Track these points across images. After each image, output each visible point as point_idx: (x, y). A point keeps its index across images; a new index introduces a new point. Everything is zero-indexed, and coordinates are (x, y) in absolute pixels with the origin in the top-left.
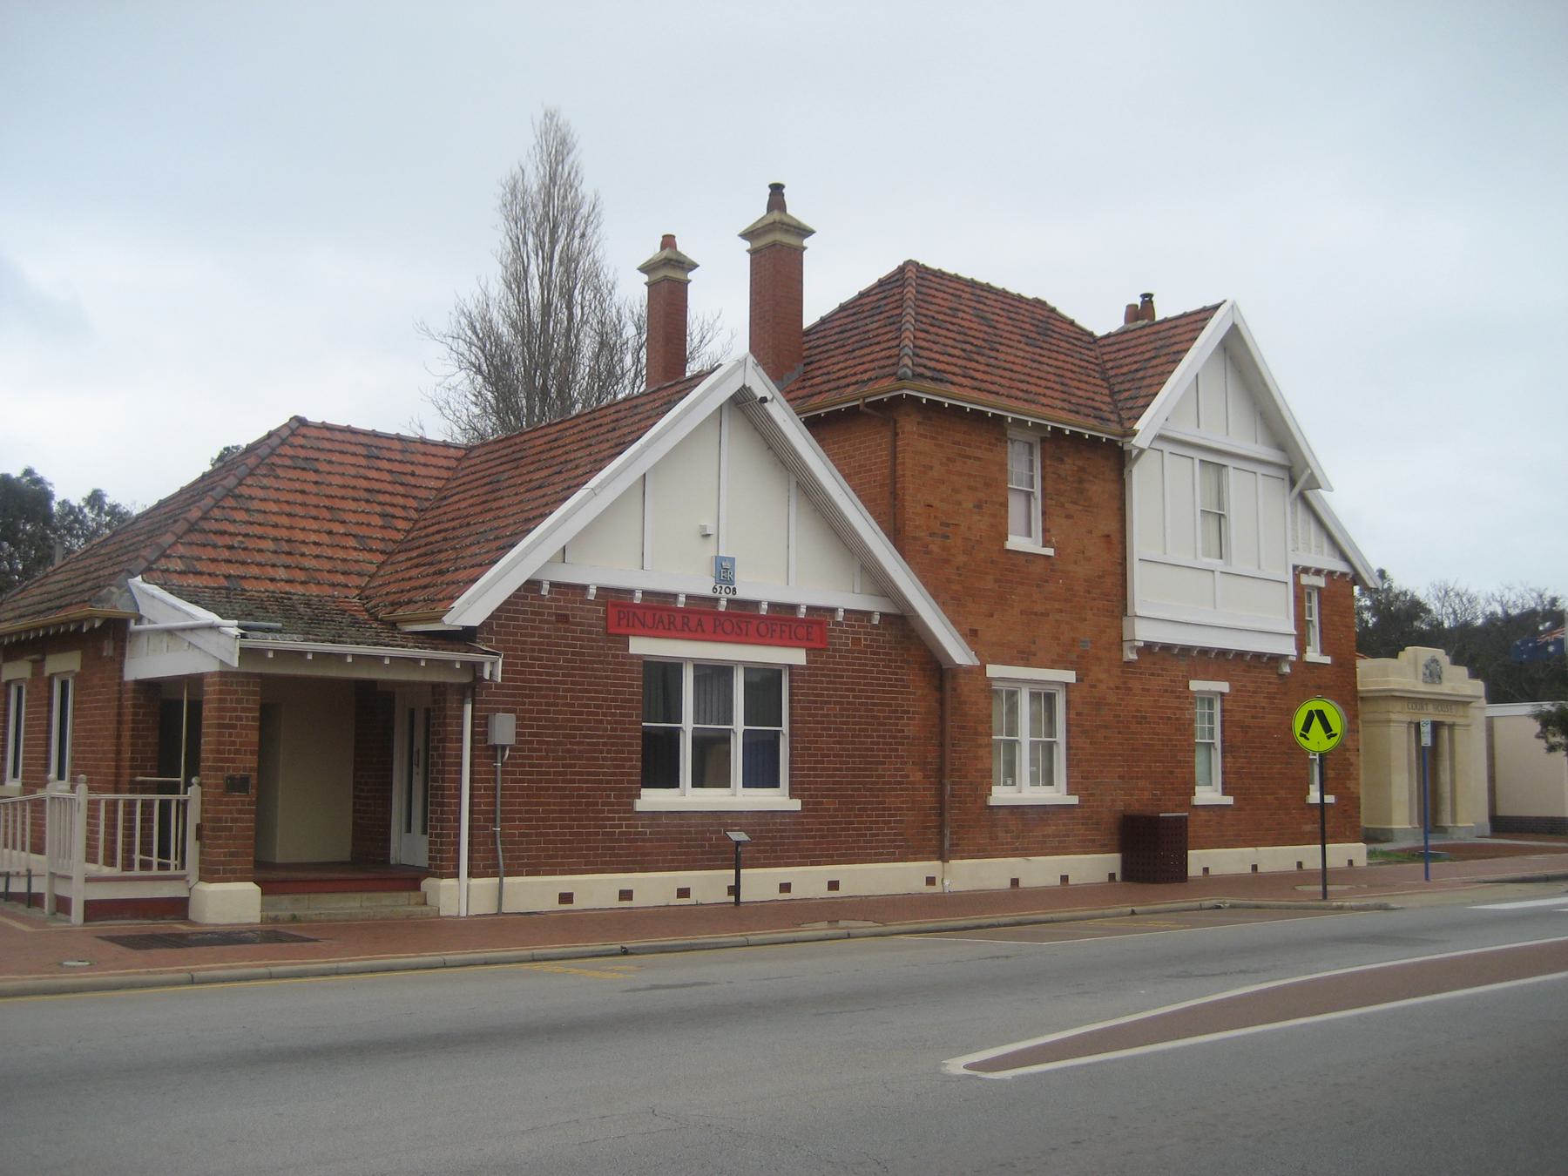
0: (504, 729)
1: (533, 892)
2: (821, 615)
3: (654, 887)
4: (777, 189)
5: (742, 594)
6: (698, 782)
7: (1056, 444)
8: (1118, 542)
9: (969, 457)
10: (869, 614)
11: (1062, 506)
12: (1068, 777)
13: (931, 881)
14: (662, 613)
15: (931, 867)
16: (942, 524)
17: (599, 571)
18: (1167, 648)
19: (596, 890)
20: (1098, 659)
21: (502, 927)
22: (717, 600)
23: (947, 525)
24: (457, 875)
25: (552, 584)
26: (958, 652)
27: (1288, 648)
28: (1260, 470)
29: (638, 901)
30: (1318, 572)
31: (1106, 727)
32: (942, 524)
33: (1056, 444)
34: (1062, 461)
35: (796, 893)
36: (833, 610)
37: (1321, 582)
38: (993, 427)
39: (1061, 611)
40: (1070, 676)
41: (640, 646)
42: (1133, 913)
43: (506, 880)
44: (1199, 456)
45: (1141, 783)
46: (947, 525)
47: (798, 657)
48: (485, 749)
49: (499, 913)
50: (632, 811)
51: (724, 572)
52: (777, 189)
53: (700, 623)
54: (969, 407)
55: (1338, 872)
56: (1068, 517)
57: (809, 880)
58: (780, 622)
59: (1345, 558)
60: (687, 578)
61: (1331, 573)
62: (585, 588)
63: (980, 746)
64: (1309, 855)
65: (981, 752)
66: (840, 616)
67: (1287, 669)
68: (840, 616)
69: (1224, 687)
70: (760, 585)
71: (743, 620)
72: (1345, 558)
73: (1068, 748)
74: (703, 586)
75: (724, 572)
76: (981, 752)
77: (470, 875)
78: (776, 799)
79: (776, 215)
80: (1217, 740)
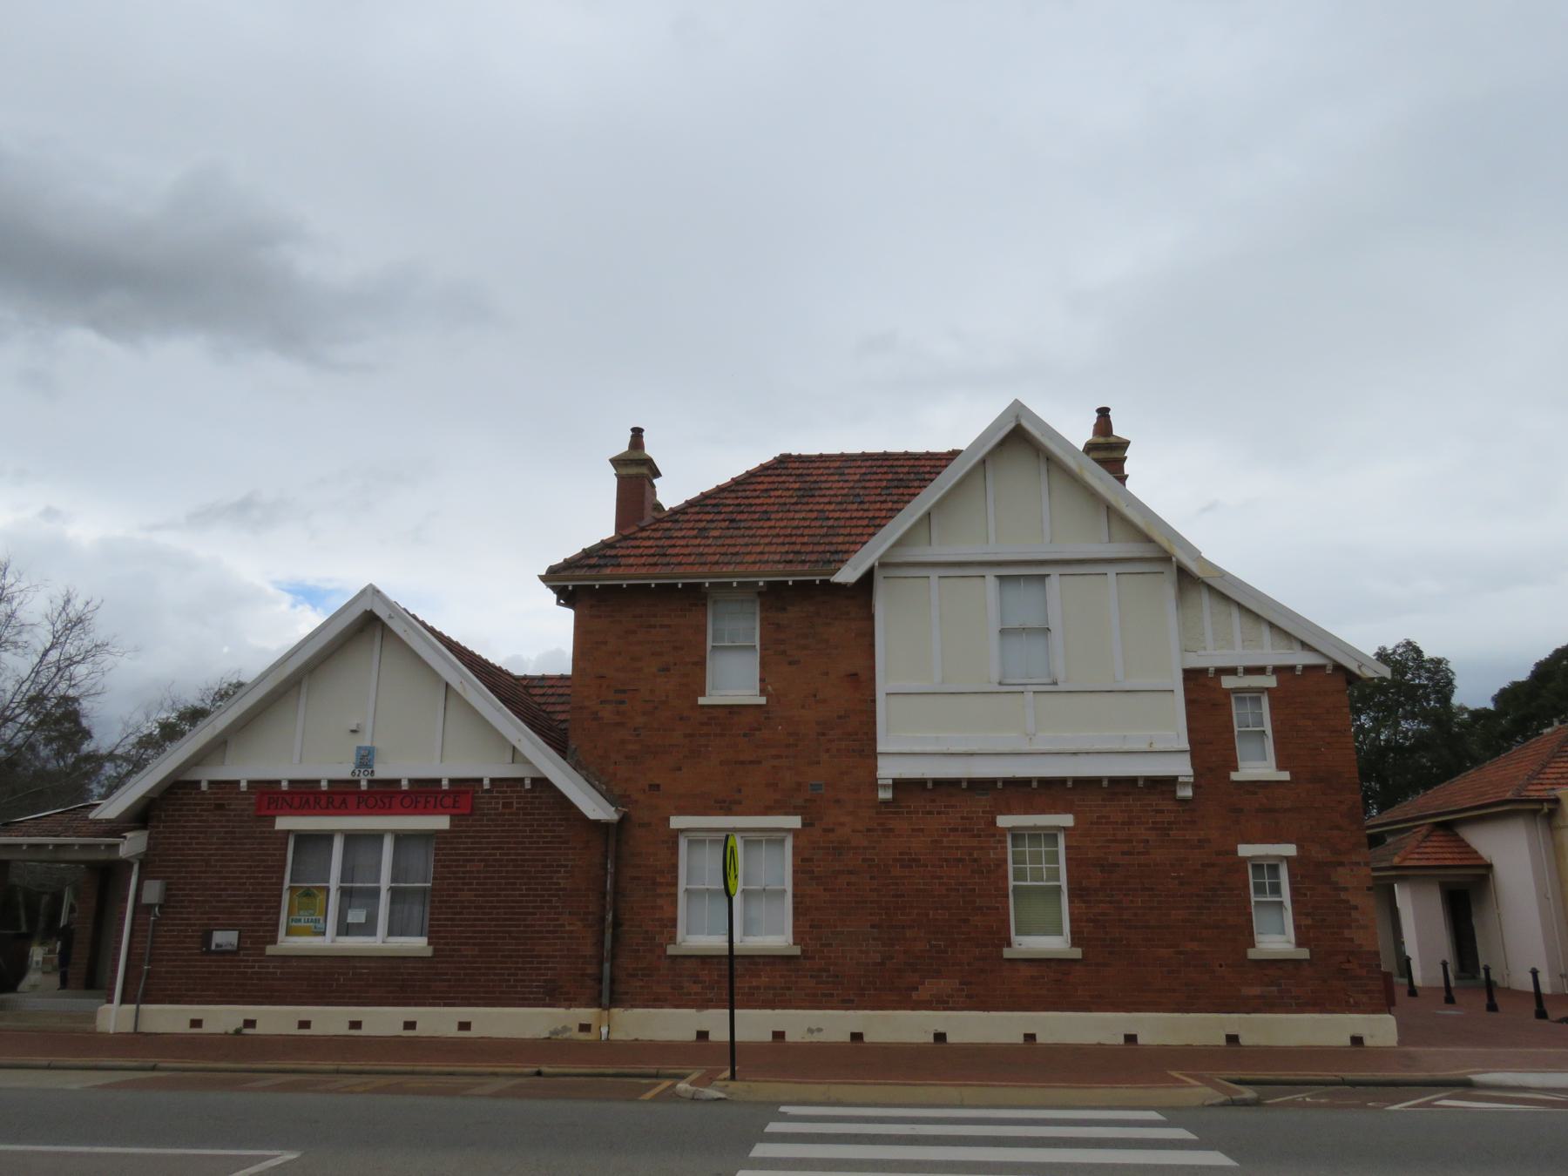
0: (153, 892)
1: (168, 1018)
2: (464, 788)
3: (275, 1019)
4: (637, 433)
5: (382, 772)
6: (391, 933)
7: (774, 596)
8: (862, 682)
9: (650, 626)
10: (521, 780)
11: (784, 652)
12: (795, 926)
13: (585, 1028)
14: (306, 796)
15: (586, 1014)
16: (617, 691)
17: (243, 769)
18: (954, 783)
19: (222, 1018)
20: (838, 801)
21: (137, 1042)
22: (358, 782)
23: (624, 691)
24: (111, 1001)
25: (211, 783)
26: (594, 807)
27: (1181, 767)
28: (1111, 570)
29: (207, 1028)
30: (1260, 670)
31: (850, 872)
32: (617, 691)
33: (774, 596)
34: (784, 609)
35: (422, 1030)
36: (480, 780)
37: (1270, 681)
38: (694, 596)
39: (780, 757)
40: (795, 822)
41: (283, 823)
42: (539, 1074)
43: (142, 1007)
44: (991, 574)
45: (909, 933)
46: (624, 691)
47: (441, 822)
48: (141, 909)
49: (136, 1032)
50: (263, 954)
51: (365, 759)
52: (637, 433)
53: (344, 801)
54: (625, 583)
55: (756, 1048)
56: (790, 663)
57: (438, 1021)
58: (424, 794)
59: (1305, 645)
60: (332, 766)
61: (1277, 670)
62: (238, 782)
63: (660, 896)
64: (714, 1021)
65: (660, 902)
66: (486, 784)
67: (1187, 793)
68: (486, 784)
69: (1067, 820)
70: (399, 767)
71: (386, 796)
72: (1305, 645)
73: (794, 896)
74: (344, 771)
75: (365, 759)
76: (660, 902)
77: (123, 1001)
78: (417, 944)
79: (636, 455)
80: (1063, 882)
